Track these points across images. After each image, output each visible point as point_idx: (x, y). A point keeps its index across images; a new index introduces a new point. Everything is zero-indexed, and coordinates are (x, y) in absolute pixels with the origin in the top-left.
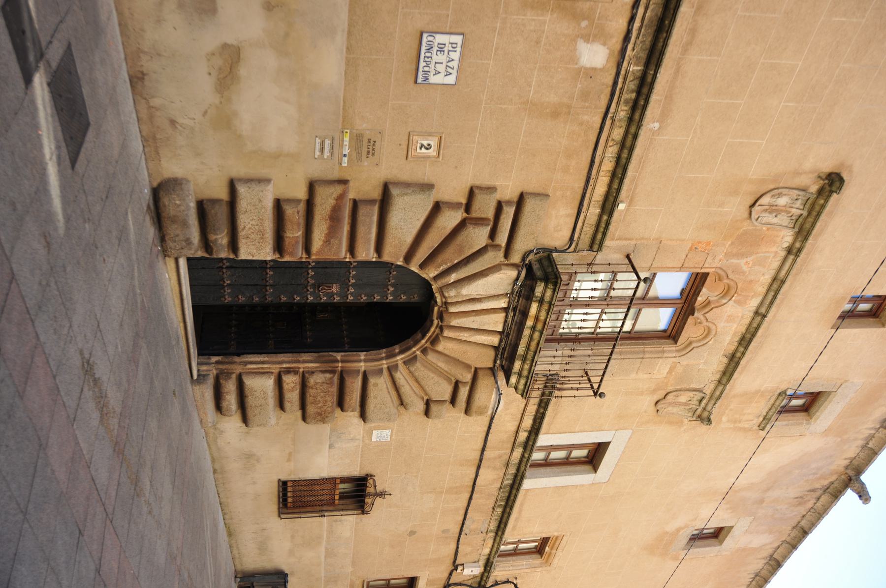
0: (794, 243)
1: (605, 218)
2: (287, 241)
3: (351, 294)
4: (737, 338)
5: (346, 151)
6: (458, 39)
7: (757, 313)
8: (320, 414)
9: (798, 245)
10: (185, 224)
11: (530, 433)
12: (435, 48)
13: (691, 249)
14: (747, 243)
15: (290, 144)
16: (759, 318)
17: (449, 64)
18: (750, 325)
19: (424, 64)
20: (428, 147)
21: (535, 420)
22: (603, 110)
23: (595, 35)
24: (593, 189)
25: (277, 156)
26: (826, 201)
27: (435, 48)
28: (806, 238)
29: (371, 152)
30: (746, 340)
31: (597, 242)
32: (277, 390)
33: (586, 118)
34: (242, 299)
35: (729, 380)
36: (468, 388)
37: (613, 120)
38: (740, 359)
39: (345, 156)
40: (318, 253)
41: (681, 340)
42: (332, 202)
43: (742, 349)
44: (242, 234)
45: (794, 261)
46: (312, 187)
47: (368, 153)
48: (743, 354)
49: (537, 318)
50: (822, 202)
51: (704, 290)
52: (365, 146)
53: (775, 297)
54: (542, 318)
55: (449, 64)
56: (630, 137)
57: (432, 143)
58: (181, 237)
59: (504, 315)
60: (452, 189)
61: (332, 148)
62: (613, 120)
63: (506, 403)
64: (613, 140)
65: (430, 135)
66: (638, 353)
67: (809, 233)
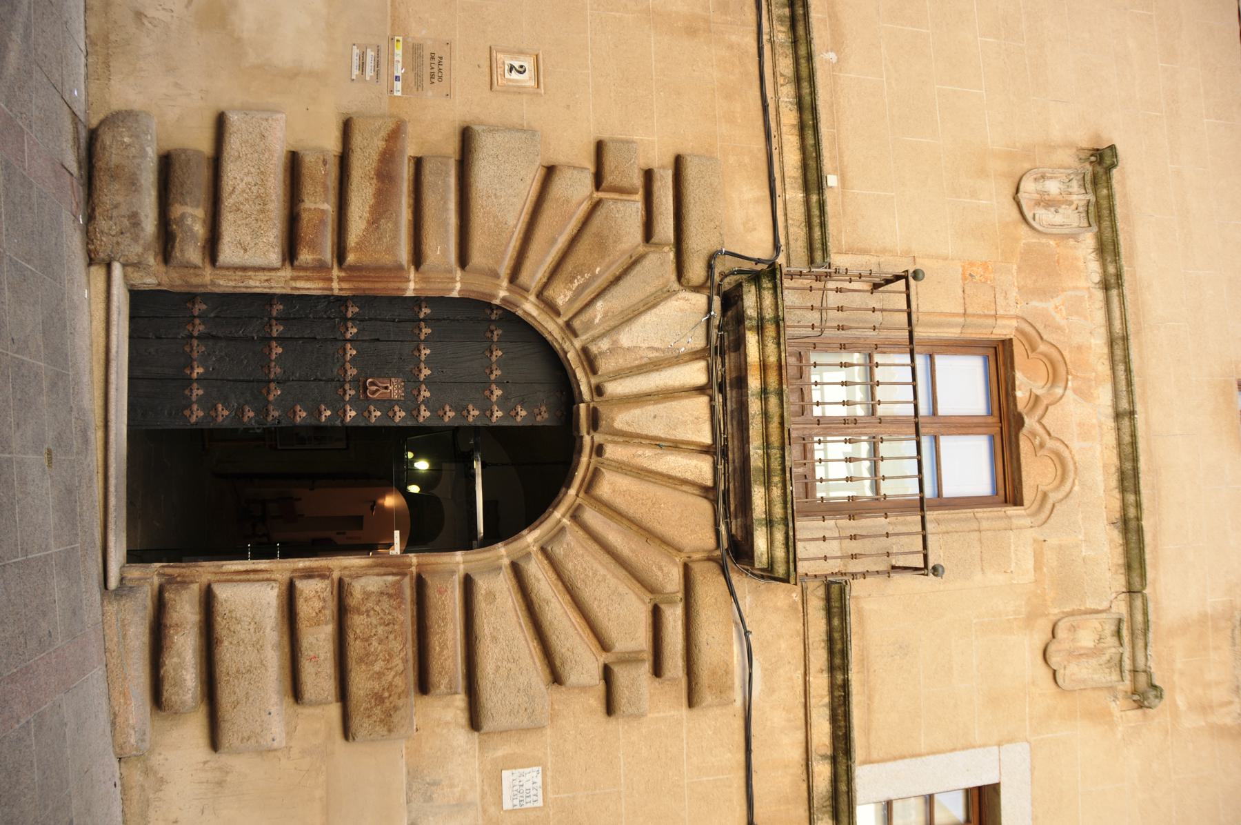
0: (1105, 271)
1: (814, 198)
2: (305, 216)
3: (426, 402)
4: (1114, 482)
5: (399, 71)
7: (1118, 416)
8: (379, 699)
9: (1111, 269)
10: (133, 184)
11: (834, 760)
13: (964, 279)
14: (1043, 271)
15: (314, 55)
16: (1126, 422)
18: (1119, 444)
20: (522, 70)
21: (834, 719)
22: (754, 28)
24: (781, 154)
25: (294, 74)
26: (1110, 188)
28: (1116, 254)
29: (436, 76)
30: (1128, 478)
31: (818, 245)
32: (285, 628)
34: (223, 413)
35: (1143, 576)
37: (772, 42)
38: (1138, 519)
39: (397, 78)
40: (360, 246)
41: (1028, 493)
42: (379, 144)
43: (1131, 498)
44: (228, 202)
45: (1121, 296)
46: (347, 128)
48: (1138, 505)
49: (764, 367)
50: (1105, 192)
51: (1019, 376)
52: (429, 67)
53: (1128, 371)
54: (772, 359)
56: (803, 62)
57: (526, 65)
58: (123, 210)
59: (705, 399)
61: (378, 64)
62: (772, 42)
63: (765, 670)
64: (782, 75)
65: (521, 52)
66: (967, 520)
67: (1115, 244)
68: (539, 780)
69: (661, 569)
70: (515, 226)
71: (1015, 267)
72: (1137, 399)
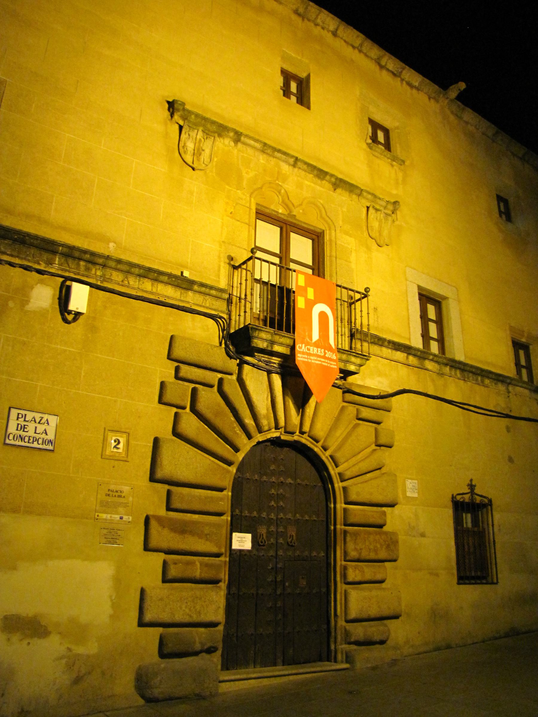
5: (117, 517)
6: (14, 413)
7: (294, 166)
8: (388, 546)
12: (21, 433)
13: (232, 217)
17: (38, 421)
19: (35, 443)
21: (397, 350)
23: (23, 294)
24: (168, 297)
27: (21, 433)
30: (321, 174)
33: (99, 303)
36: (362, 409)
38: (337, 178)
45: (246, 136)
47: (120, 496)
55: (38, 421)
57: (114, 438)
60: (161, 421)
64: (122, 281)
66: (331, 262)
68: (410, 481)
69: (349, 414)
70: (210, 460)
71: (227, 187)
72: (261, 139)
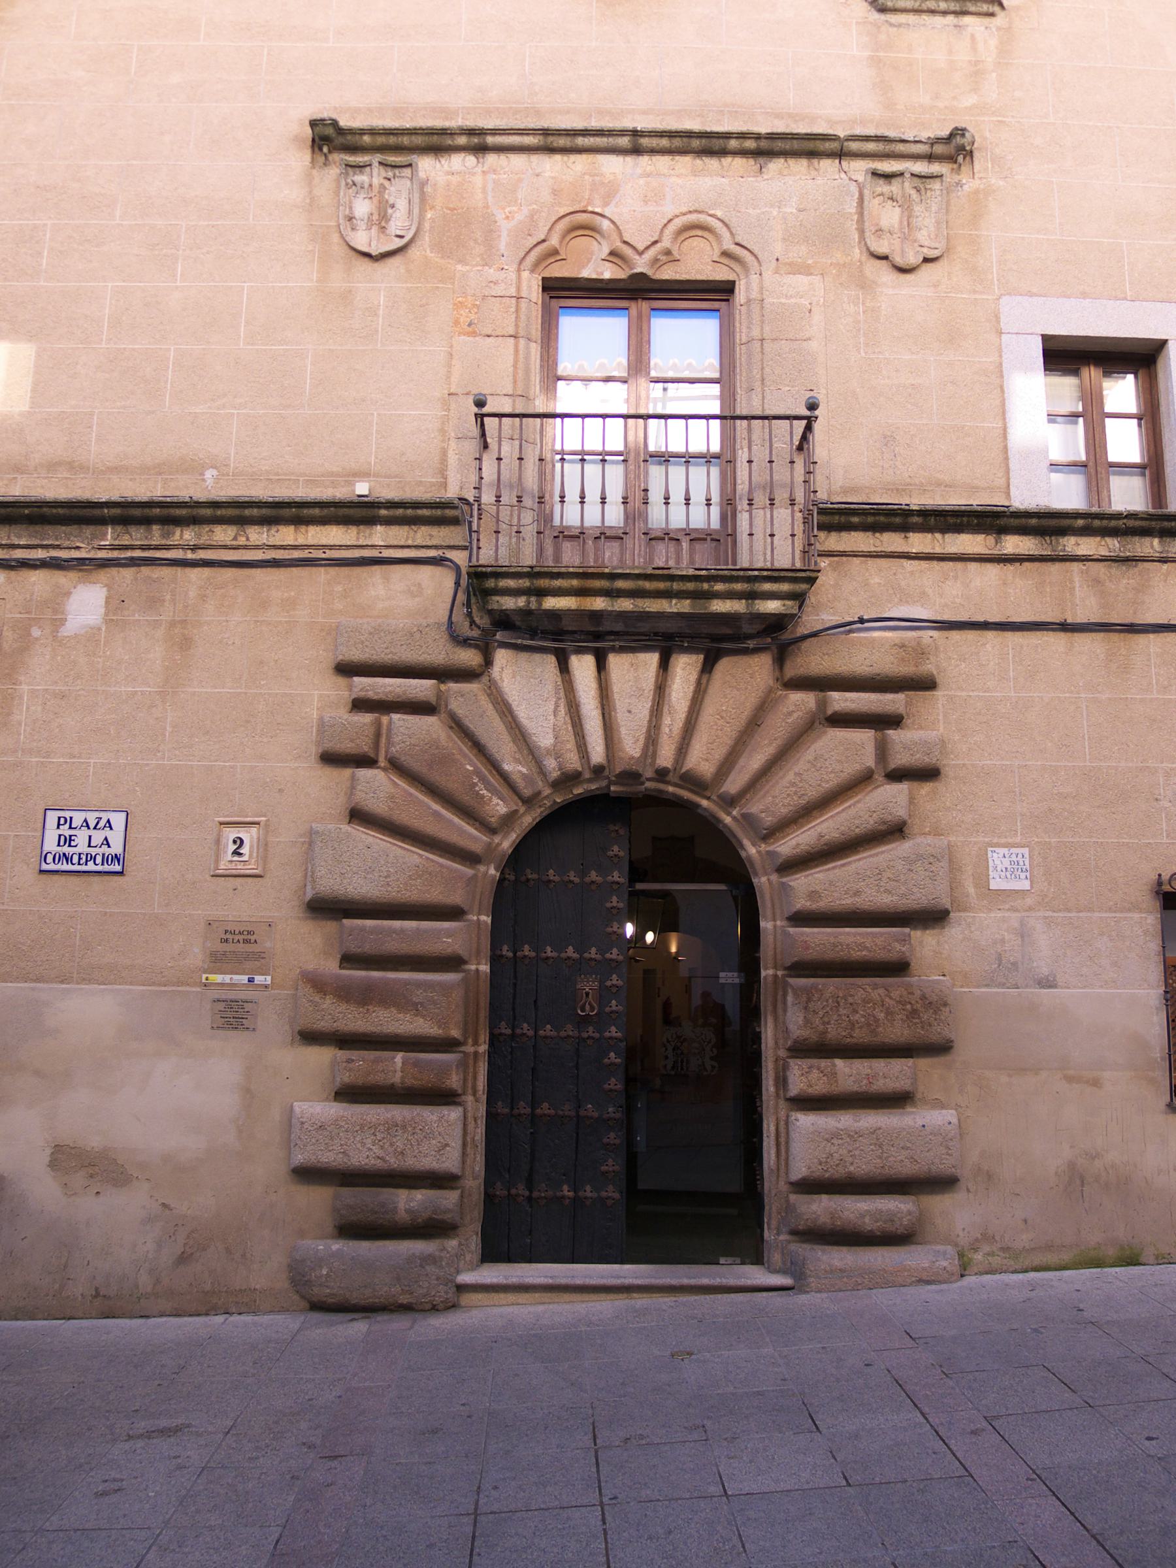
2: (410, 1082)
3: (601, 951)
4: (712, 163)
5: (244, 979)
6: (52, 817)
7: (636, 151)
12: (66, 849)
13: (474, 334)
14: (463, 231)
17: (92, 826)
19: (91, 863)
20: (239, 842)
21: (958, 529)
23: (54, 611)
26: (362, 132)
27: (66, 849)
28: (444, 132)
29: (247, 936)
30: (709, 145)
33: (192, 594)
35: (825, 138)
36: (835, 695)
38: (758, 137)
41: (721, 274)
42: (328, 1002)
44: (394, 1162)
45: (495, 132)
46: (310, 1037)
47: (246, 941)
48: (742, 136)
50: (367, 139)
51: (586, 273)
53: (585, 133)
55: (92, 826)
60: (327, 789)
62: (194, 548)
64: (235, 539)
65: (218, 842)
68: (1002, 851)
69: (790, 714)
70: (421, 856)
71: (459, 267)
